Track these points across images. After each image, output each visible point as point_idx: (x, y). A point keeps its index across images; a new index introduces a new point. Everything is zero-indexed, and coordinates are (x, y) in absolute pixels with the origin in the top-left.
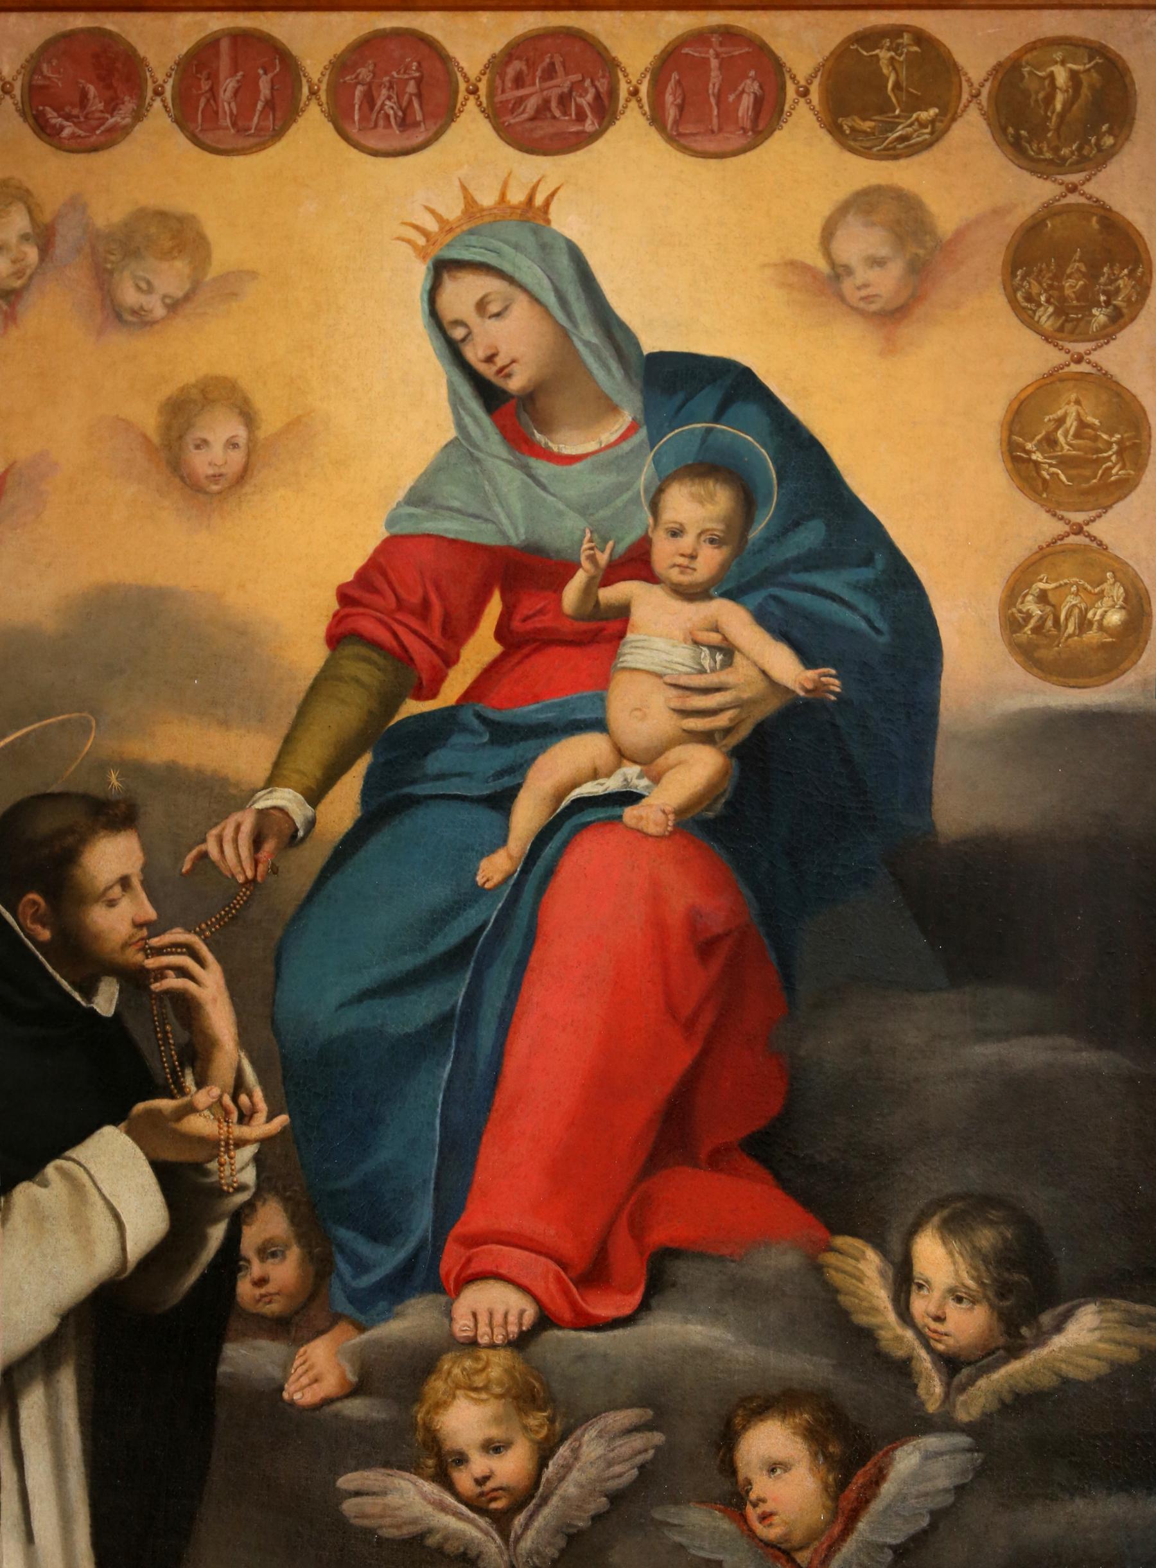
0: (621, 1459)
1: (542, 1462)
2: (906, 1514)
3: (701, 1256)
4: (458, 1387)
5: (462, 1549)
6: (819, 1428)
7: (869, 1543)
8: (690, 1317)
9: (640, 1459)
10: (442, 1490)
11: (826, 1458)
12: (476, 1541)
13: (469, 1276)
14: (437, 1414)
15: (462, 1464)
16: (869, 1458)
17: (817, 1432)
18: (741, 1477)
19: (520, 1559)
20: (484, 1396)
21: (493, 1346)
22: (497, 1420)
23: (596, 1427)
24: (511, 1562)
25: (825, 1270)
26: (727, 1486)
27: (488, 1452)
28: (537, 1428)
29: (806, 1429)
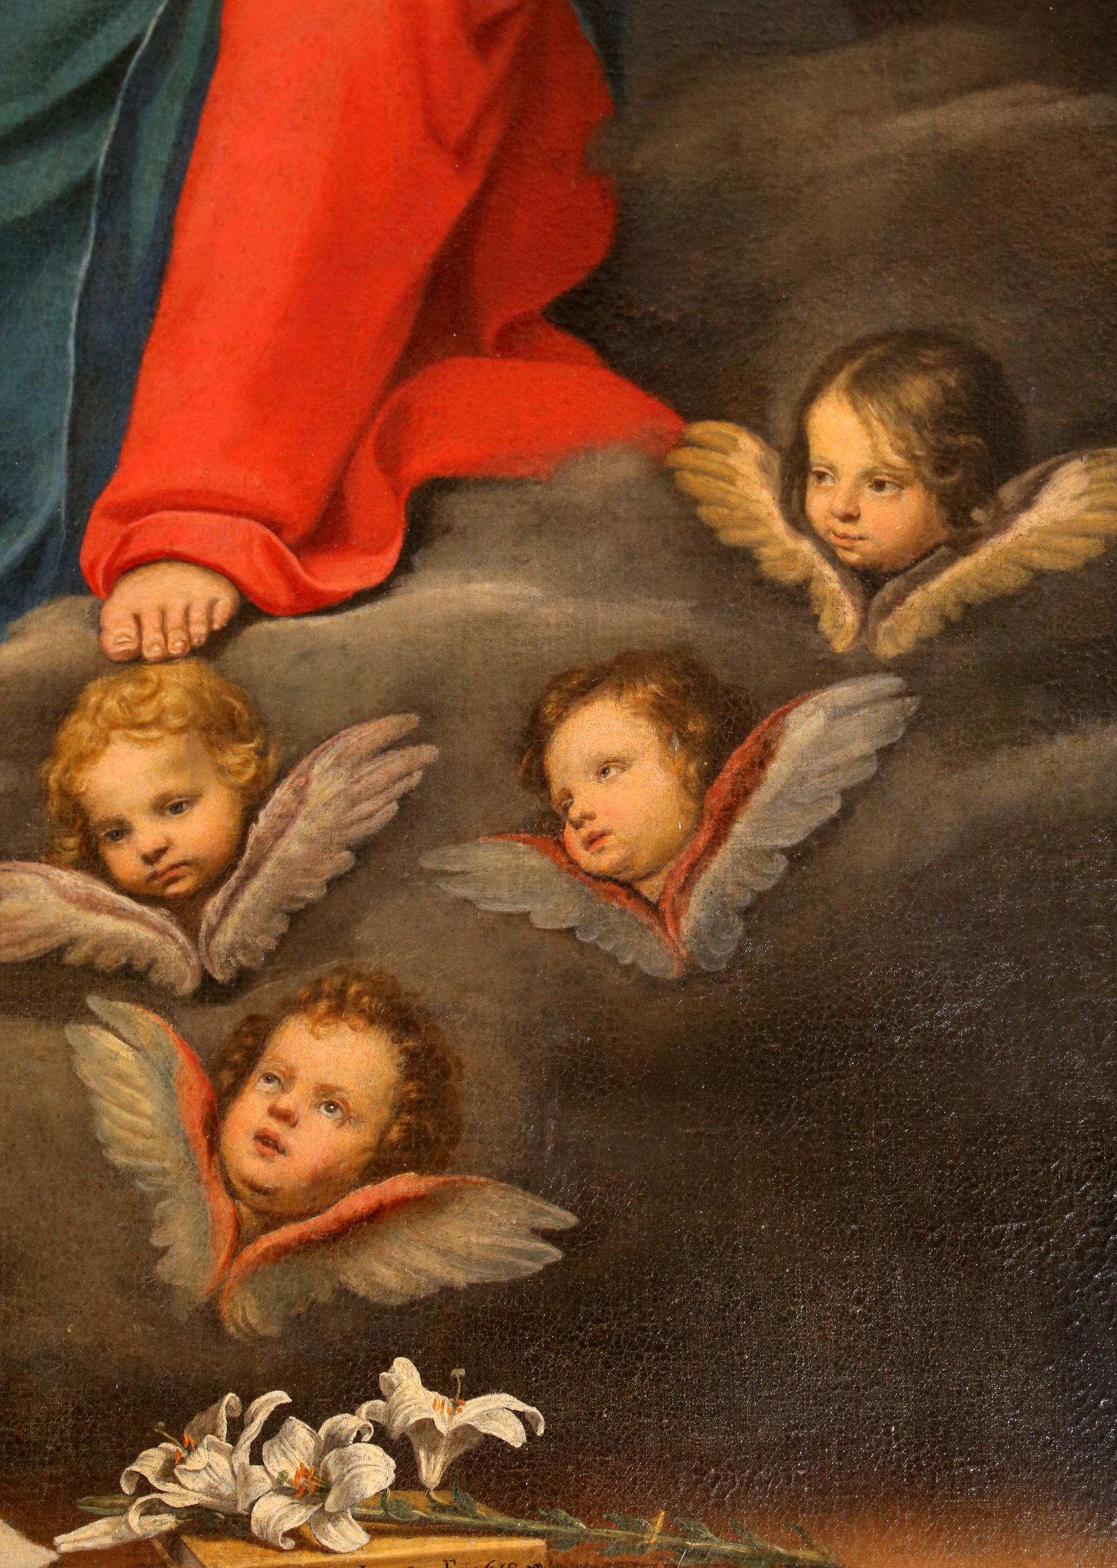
0: (371, 792)
1: (249, 817)
2: (806, 800)
3: (488, 483)
4: (113, 726)
5: (124, 960)
6: (673, 701)
7: (750, 851)
8: (473, 572)
9: (400, 788)
10: (91, 879)
11: (683, 741)
12: (147, 945)
13: (127, 563)
14: (80, 770)
15: (122, 837)
16: (747, 731)
17: (670, 706)
18: (555, 790)
19: (216, 960)
20: (154, 733)
21: (167, 659)
22: (177, 765)
23: (331, 752)
24: (202, 966)
25: (678, 474)
26: (536, 805)
27: (162, 814)
28: (239, 768)
29: (653, 706)
